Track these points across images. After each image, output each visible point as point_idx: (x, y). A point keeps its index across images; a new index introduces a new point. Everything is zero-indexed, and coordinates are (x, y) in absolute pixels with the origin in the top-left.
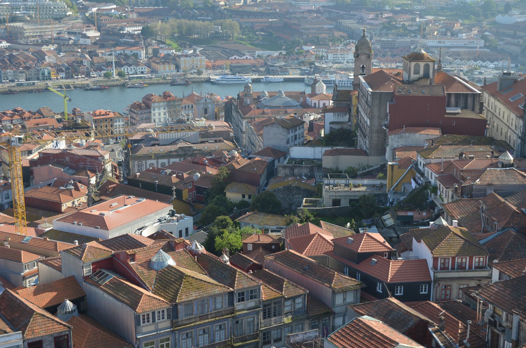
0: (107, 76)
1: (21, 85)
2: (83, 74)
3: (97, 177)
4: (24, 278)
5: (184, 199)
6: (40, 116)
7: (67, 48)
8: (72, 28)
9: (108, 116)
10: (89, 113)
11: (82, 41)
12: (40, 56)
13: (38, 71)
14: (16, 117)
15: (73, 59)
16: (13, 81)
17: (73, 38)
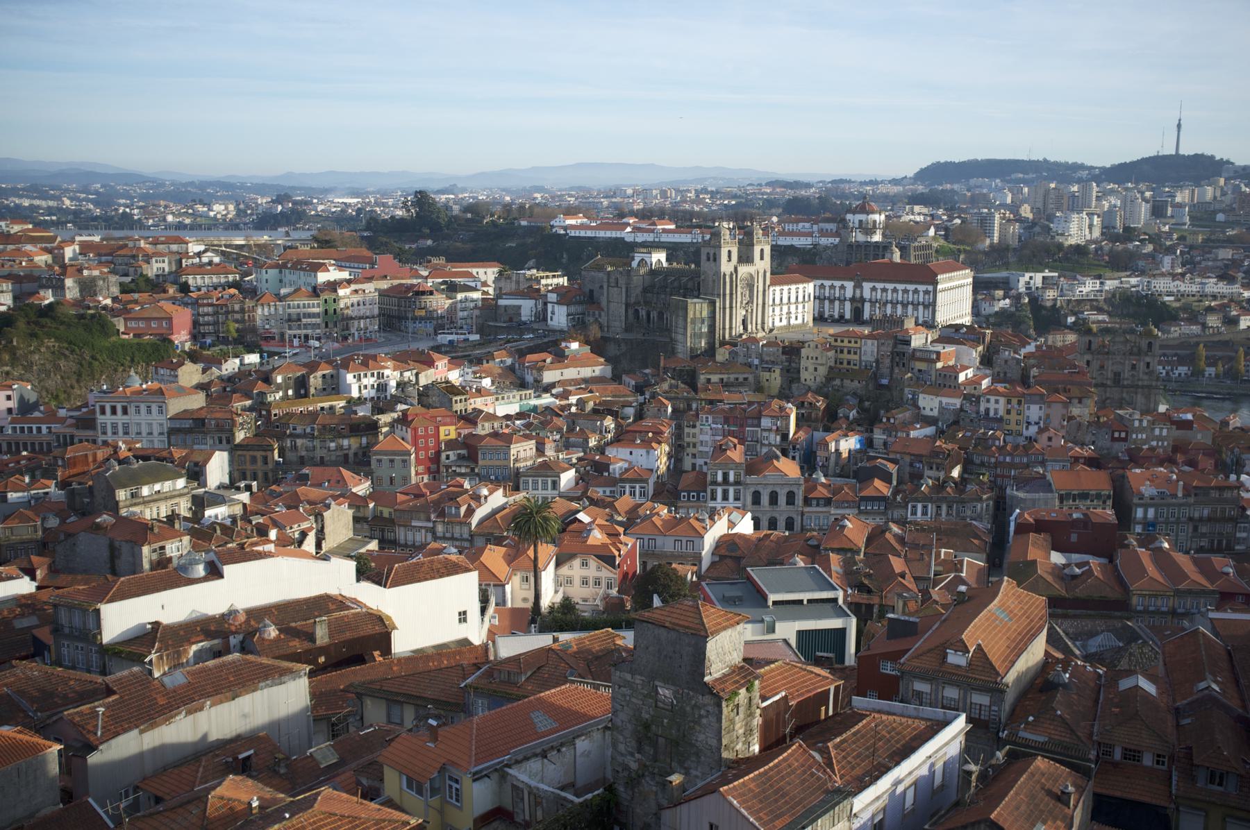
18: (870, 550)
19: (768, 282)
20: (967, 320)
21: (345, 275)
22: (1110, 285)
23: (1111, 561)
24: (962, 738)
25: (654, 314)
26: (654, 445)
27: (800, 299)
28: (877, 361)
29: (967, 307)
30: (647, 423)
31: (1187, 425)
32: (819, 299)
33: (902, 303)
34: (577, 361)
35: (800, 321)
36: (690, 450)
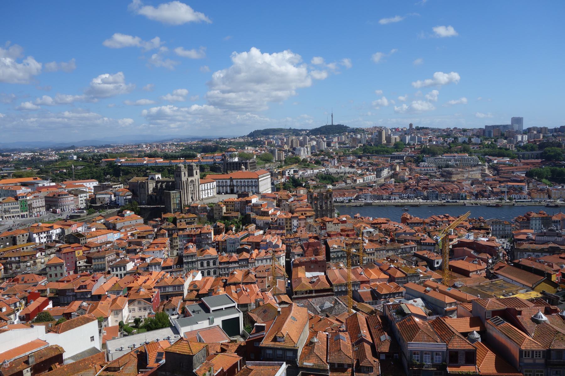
5: (553, 280)
15: (480, 189)
16: (444, 199)
18: (245, 281)
21: (29, 190)
22: (316, 171)
23: (325, 274)
24: (285, 371)
25: (158, 197)
29: (269, 185)
31: (344, 222)
32: (218, 186)
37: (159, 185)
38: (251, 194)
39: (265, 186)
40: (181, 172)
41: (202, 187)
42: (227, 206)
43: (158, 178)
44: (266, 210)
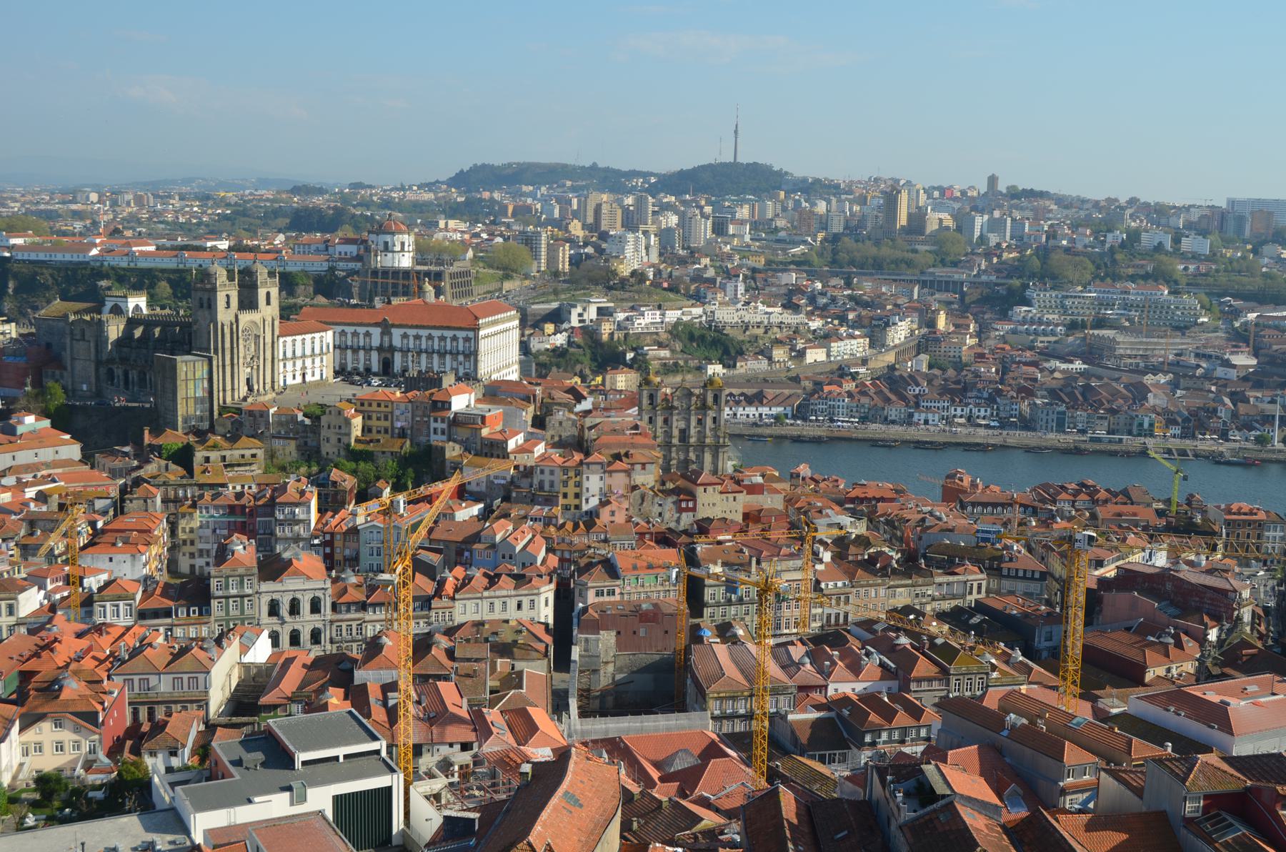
0: (1261, 441)
1: (1098, 440)
2: (1214, 433)
3: (1221, 630)
4: (1063, 792)
6: (1125, 500)
7: (1190, 383)
8: (1205, 347)
9: (1254, 517)
10: (1218, 507)
11: (1220, 372)
12: (1140, 393)
13: (1132, 418)
14: (1083, 497)
15: (1198, 402)
16: (1083, 432)
17: (1204, 365)
19: (277, 333)
20: (513, 375)
25: (133, 375)
26: (140, 547)
27: (317, 351)
28: (412, 428)
30: (128, 521)
32: (340, 347)
33: (438, 352)
34: (36, 439)
35: (317, 377)
36: (188, 549)
37: (138, 333)
38: (448, 380)
39: (500, 352)
40: (214, 290)
41: (287, 344)
42: (368, 417)
43: (137, 307)
44: (499, 437)
